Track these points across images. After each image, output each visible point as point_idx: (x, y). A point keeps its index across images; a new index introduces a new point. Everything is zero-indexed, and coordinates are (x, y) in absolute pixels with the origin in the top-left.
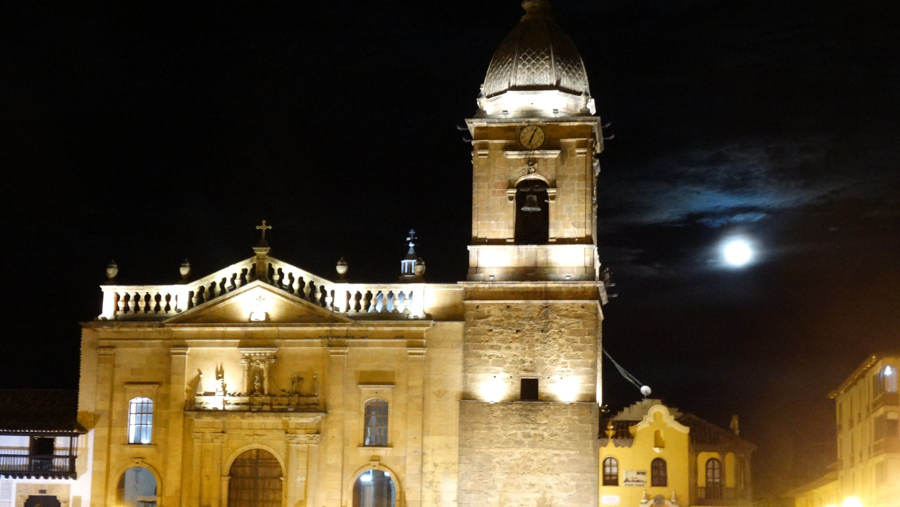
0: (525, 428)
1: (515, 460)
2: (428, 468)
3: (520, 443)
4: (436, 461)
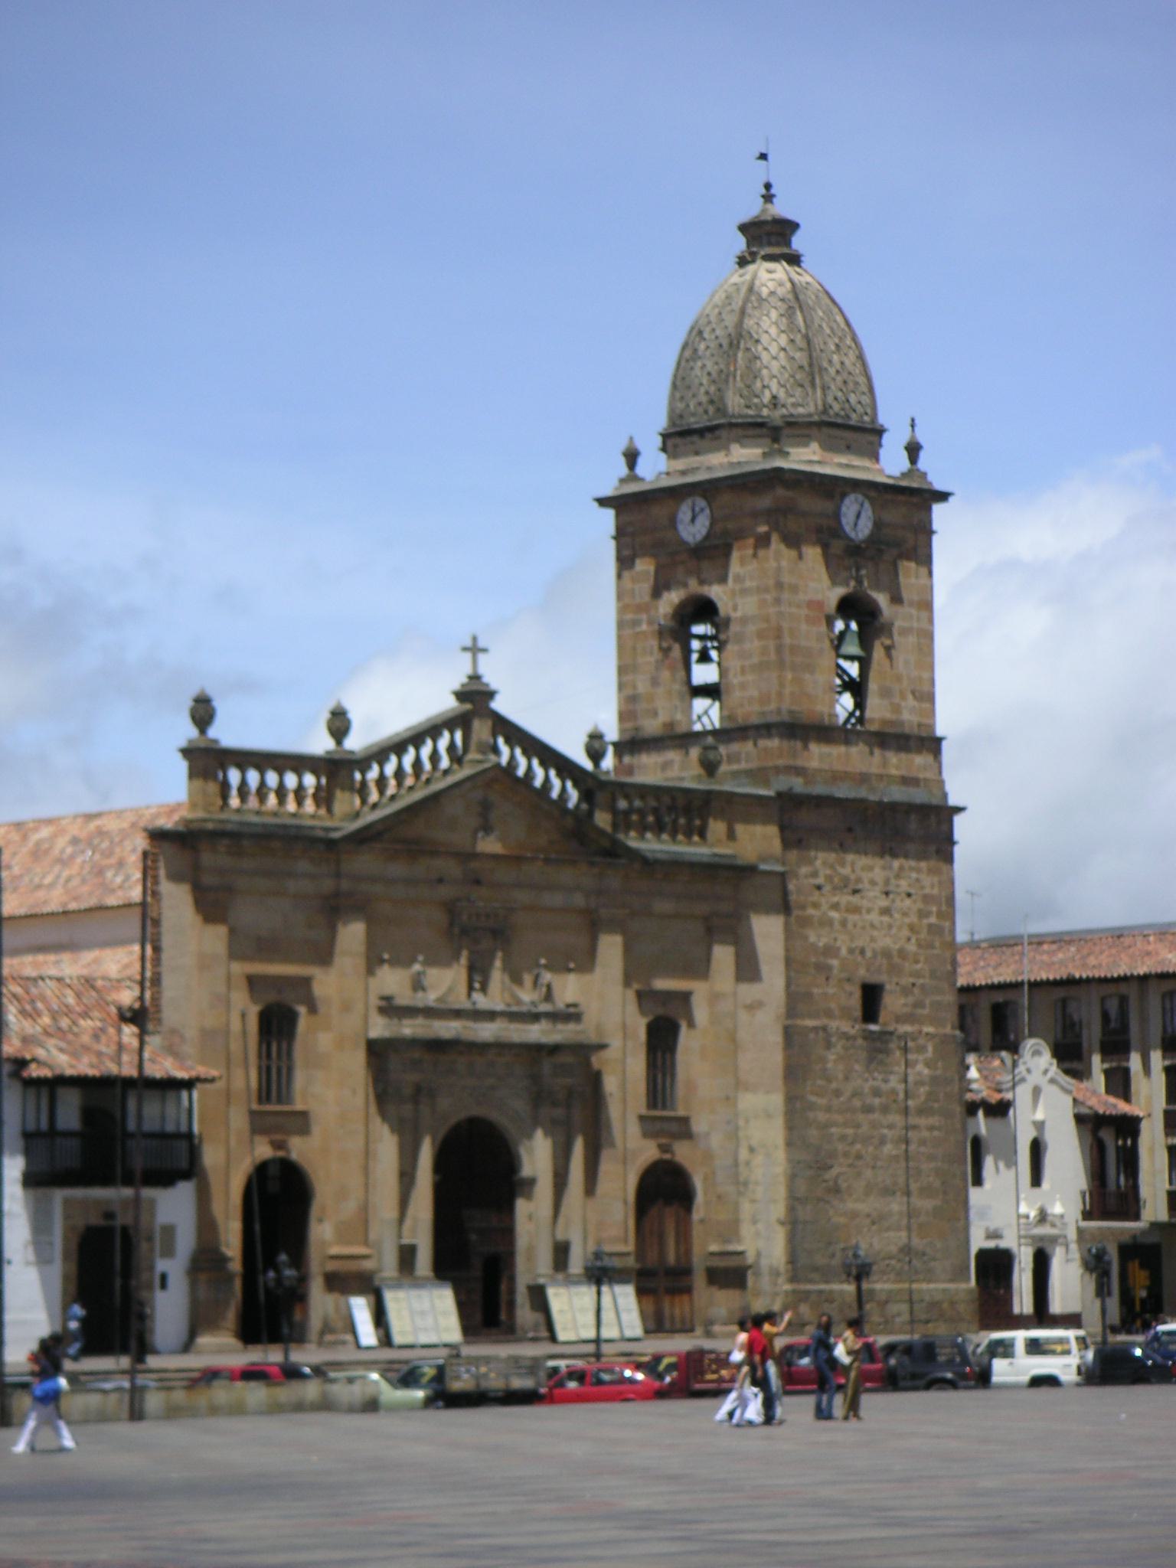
0: (874, 1079)
1: (866, 1140)
2: (743, 1154)
3: (868, 1109)
4: (754, 1143)
